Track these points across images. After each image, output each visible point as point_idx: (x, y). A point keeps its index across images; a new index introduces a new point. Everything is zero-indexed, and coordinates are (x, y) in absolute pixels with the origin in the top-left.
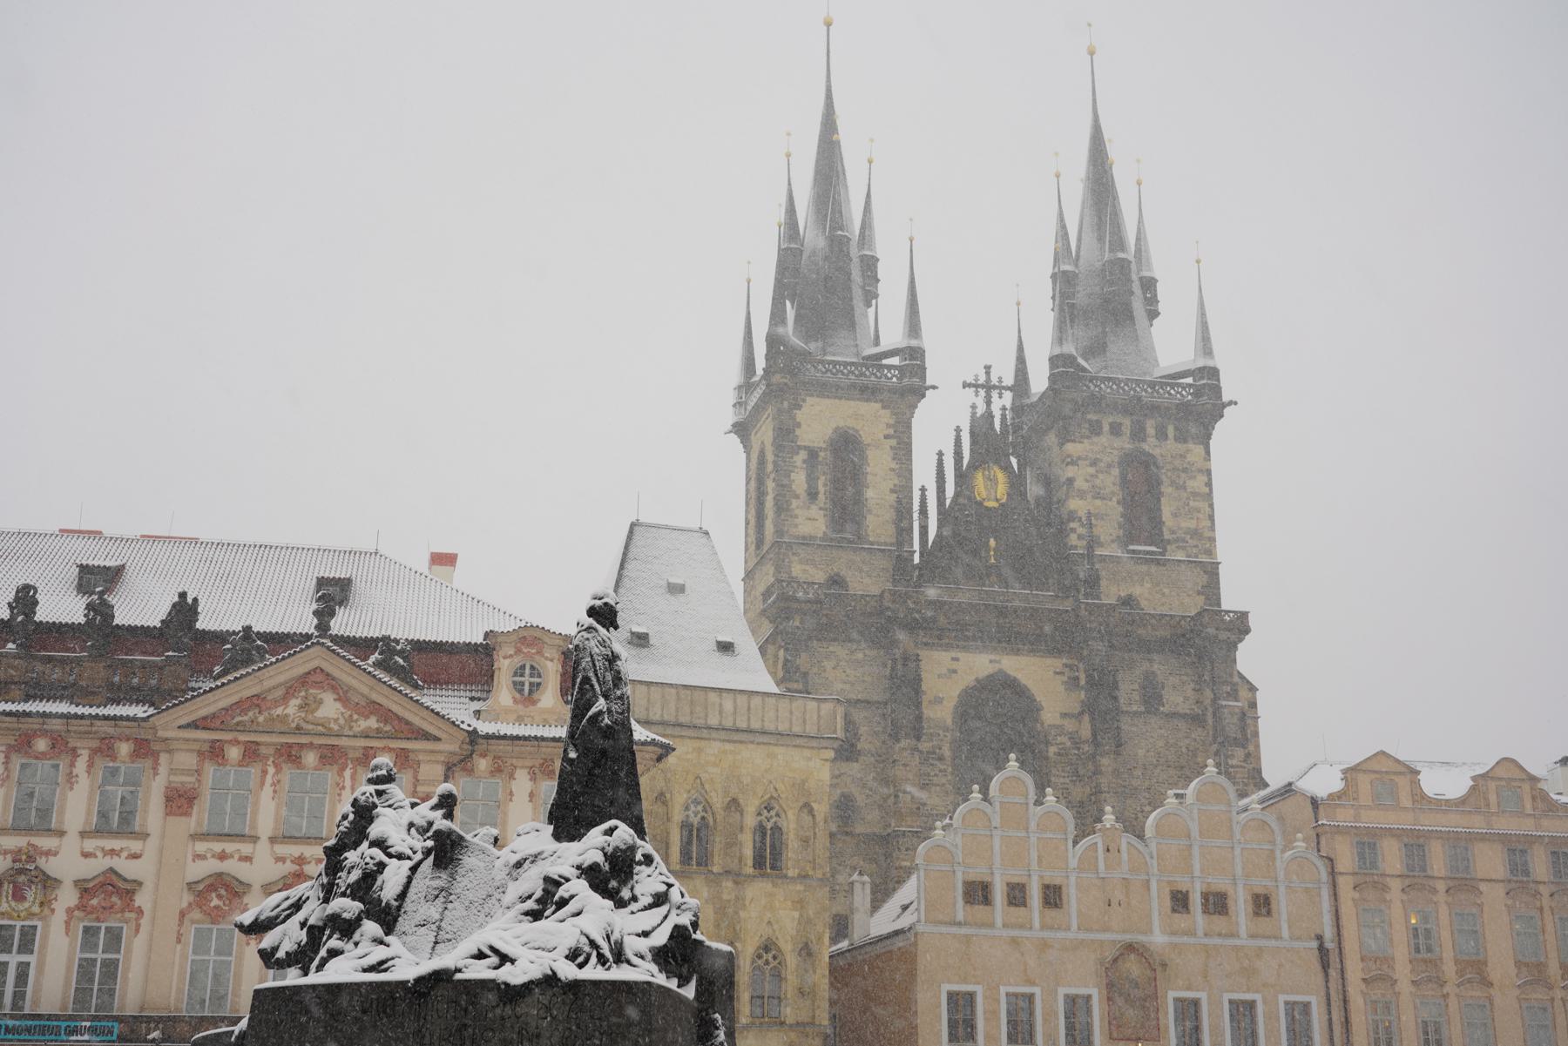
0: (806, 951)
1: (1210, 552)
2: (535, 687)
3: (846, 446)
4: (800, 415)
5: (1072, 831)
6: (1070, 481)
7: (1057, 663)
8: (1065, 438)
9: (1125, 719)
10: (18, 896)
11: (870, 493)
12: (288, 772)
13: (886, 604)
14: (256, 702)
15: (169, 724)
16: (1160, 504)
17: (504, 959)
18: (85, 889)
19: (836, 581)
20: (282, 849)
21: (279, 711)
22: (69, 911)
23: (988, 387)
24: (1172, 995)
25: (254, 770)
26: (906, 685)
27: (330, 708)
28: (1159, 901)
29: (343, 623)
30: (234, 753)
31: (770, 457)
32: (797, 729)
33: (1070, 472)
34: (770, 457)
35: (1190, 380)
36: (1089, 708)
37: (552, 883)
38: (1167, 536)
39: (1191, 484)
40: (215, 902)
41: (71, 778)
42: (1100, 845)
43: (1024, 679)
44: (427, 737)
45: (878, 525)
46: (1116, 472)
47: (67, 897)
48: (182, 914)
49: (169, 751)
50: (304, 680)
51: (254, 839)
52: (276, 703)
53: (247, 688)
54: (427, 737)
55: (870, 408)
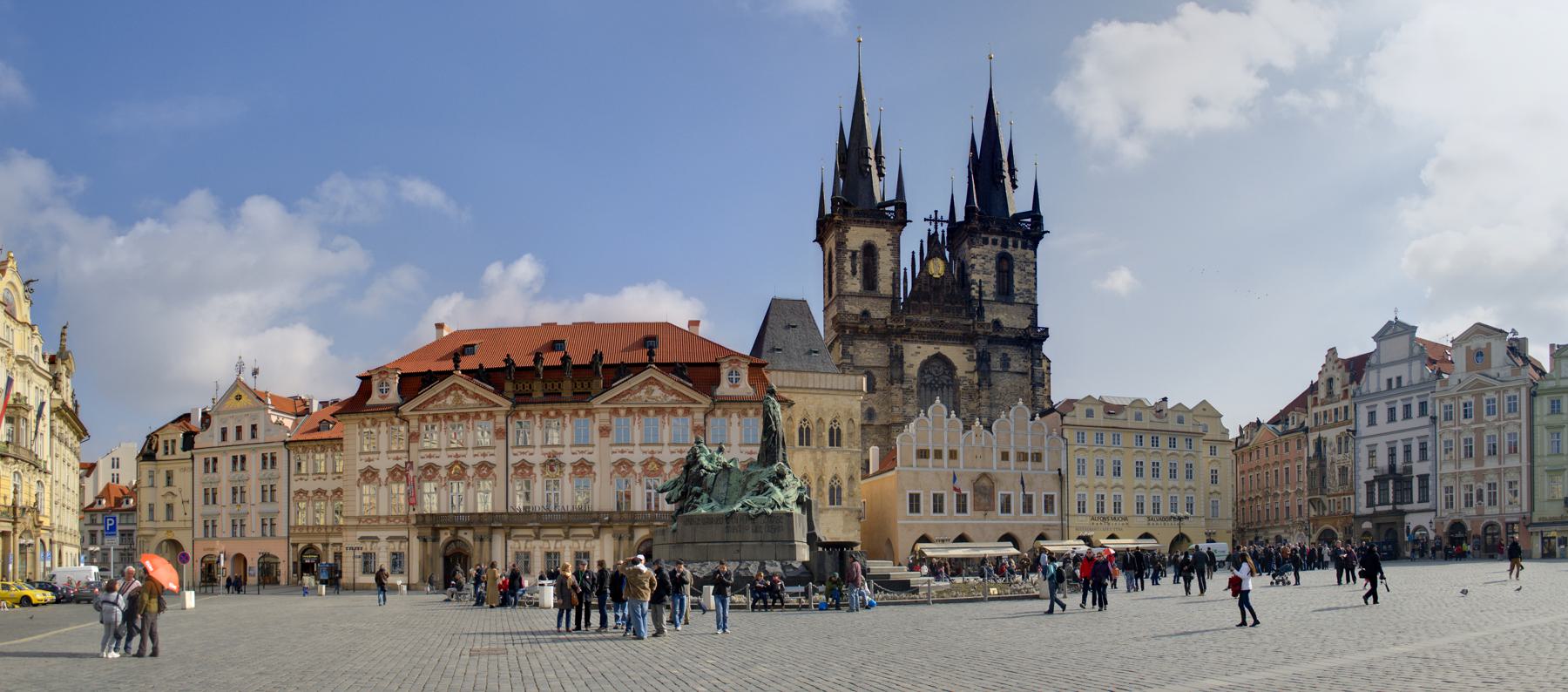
3: (869, 250)
4: (848, 235)
7: (964, 349)
11: (880, 271)
12: (644, 418)
14: (629, 391)
19: (865, 313)
20: (645, 448)
23: (936, 221)
25: (631, 418)
26: (897, 359)
27: (657, 392)
28: (995, 457)
30: (622, 412)
36: (977, 369)
43: (949, 356)
44: (695, 402)
45: (885, 286)
53: (625, 387)
54: (695, 402)
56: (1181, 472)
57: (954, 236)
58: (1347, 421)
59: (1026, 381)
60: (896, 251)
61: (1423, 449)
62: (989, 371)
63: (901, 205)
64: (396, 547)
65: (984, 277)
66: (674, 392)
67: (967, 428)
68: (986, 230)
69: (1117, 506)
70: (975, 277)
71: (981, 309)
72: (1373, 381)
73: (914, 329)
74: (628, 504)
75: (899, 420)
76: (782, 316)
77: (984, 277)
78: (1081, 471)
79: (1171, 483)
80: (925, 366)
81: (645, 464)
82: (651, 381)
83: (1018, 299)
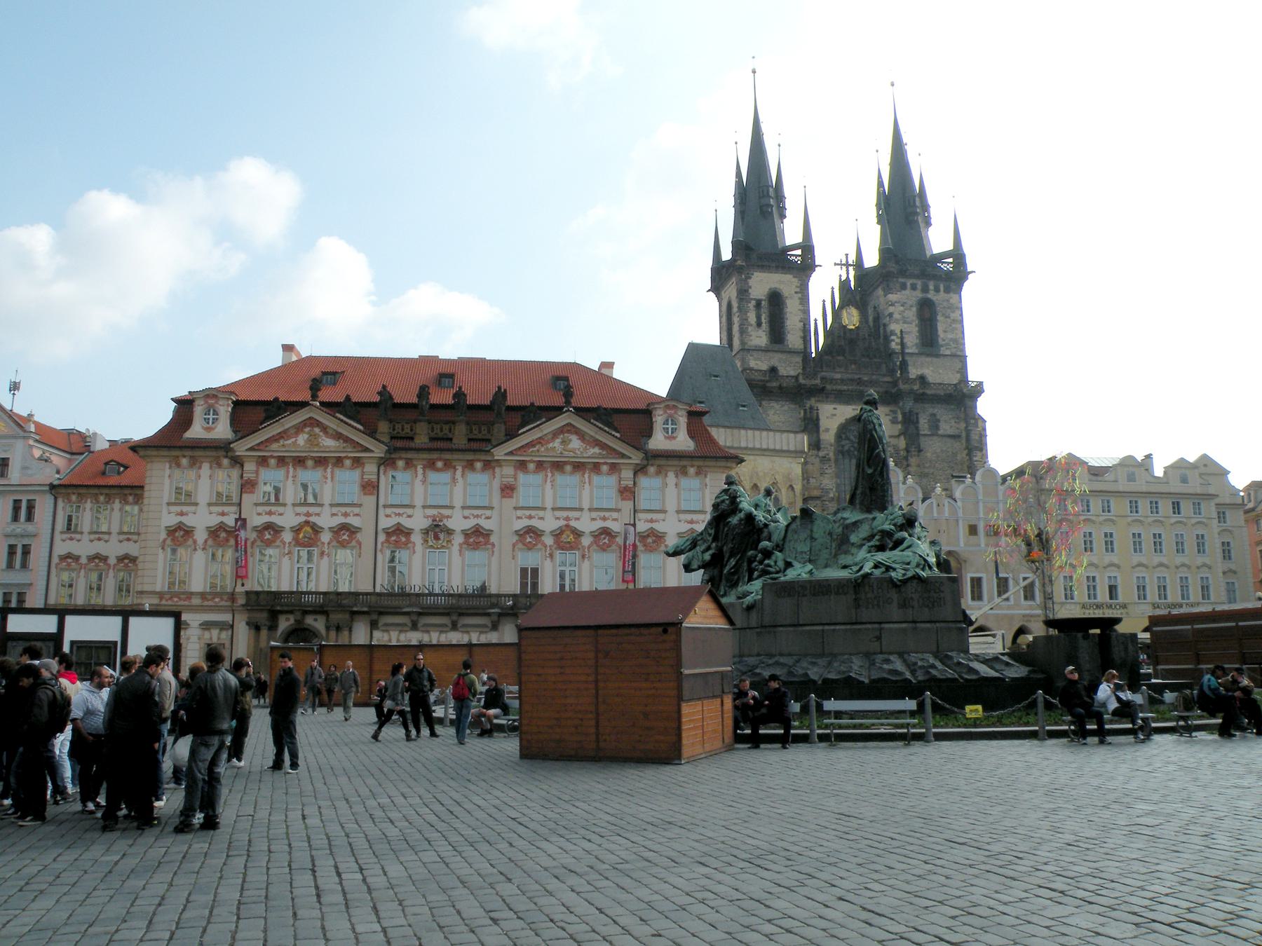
1: (963, 350)
2: (674, 430)
3: (775, 299)
4: (751, 282)
5: (921, 496)
6: (891, 315)
8: (888, 290)
9: (922, 439)
10: (437, 538)
13: (802, 381)
14: (540, 441)
15: (499, 453)
16: (937, 327)
17: (888, 568)
18: (466, 534)
19: (773, 370)
20: (558, 514)
21: (551, 445)
22: (460, 545)
23: (847, 265)
24: (969, 575)
26: (811, 424)
27: (575, 443)
28: (963, 531)
31: (735, 305)
32: (785, 448)
33: (891, 309)
34: (735, 305)
35: (951, 260)
37: (889, 534)
38: (941, 342)
39: (953, 315)
40: (529, 540)
41: (454, 480)
42: (935, 505)
44: (623, 456)
45: (793, 340)
46: (914, 309)
47: (458, 539)
48: (514, 546)
49: (501, 466)
50: (561, 431)
51: (544, 509)
52: (548, 442)
54: (623, 456)
55: (788, 277)
56: (1190, 545)
57: (862, 289)
59: (959, 445)
60: (805, 300)
62: (918, 435)
63: (807, 247)
65: (906, 327)
66: (597, 443)
68: (903, 273)
69: (1112, 590)
70: (895, 327)
71: (904, 366)
73: (829, 387)
74: (535, 585)
75: (816, 493)
77: (906, 327)
79: (1179, 559)
80: (843, 430)
81: (557, 534)
82: (570, 429)
83: (944, 351)
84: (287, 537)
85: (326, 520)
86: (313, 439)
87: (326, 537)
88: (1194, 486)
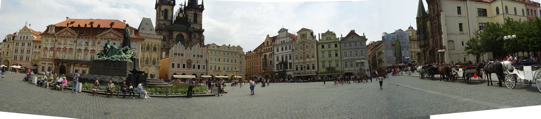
0: (158, 59)
14: (105, 34)
15: (98, 36)
18: (91, 51)
27: (112, 35)
28: (192, 56)
29: (113, 27)
45: (169, 18)
47: (90, 51)
53: (104, 33)
56: (234, 61)
58: (272, 51)
61: (290, 57)
64: (50, 66)
66: (116, 35)
67: (186, 49)
69: (219, 69)
72: (278, 42)
76: (146, 22)
78: (211, 60)
80: (177, 36)
84: (62, 50)
85: (68, 47)
86: (67, 33)
87: (68, 50)
88: (235, 51)
